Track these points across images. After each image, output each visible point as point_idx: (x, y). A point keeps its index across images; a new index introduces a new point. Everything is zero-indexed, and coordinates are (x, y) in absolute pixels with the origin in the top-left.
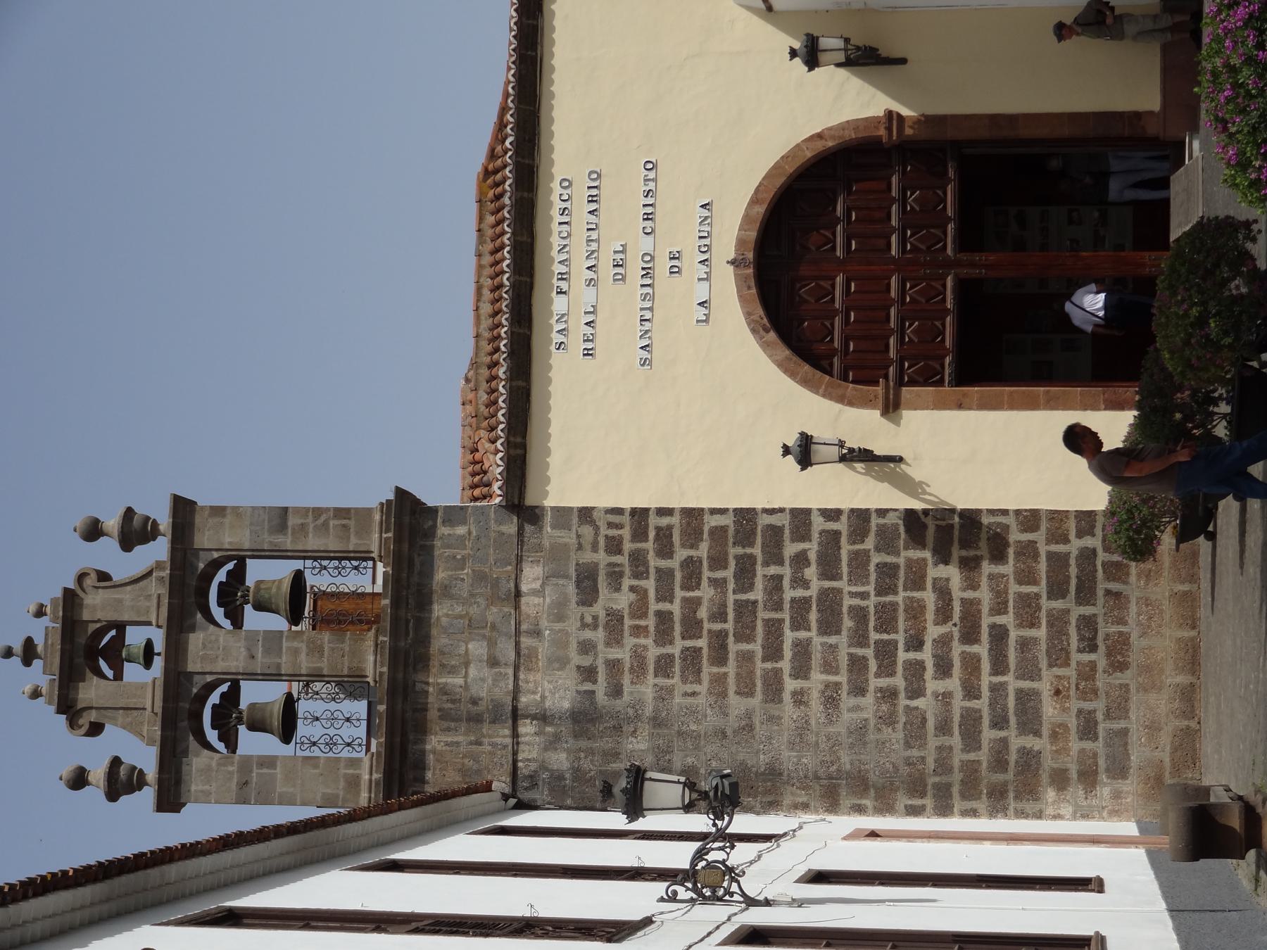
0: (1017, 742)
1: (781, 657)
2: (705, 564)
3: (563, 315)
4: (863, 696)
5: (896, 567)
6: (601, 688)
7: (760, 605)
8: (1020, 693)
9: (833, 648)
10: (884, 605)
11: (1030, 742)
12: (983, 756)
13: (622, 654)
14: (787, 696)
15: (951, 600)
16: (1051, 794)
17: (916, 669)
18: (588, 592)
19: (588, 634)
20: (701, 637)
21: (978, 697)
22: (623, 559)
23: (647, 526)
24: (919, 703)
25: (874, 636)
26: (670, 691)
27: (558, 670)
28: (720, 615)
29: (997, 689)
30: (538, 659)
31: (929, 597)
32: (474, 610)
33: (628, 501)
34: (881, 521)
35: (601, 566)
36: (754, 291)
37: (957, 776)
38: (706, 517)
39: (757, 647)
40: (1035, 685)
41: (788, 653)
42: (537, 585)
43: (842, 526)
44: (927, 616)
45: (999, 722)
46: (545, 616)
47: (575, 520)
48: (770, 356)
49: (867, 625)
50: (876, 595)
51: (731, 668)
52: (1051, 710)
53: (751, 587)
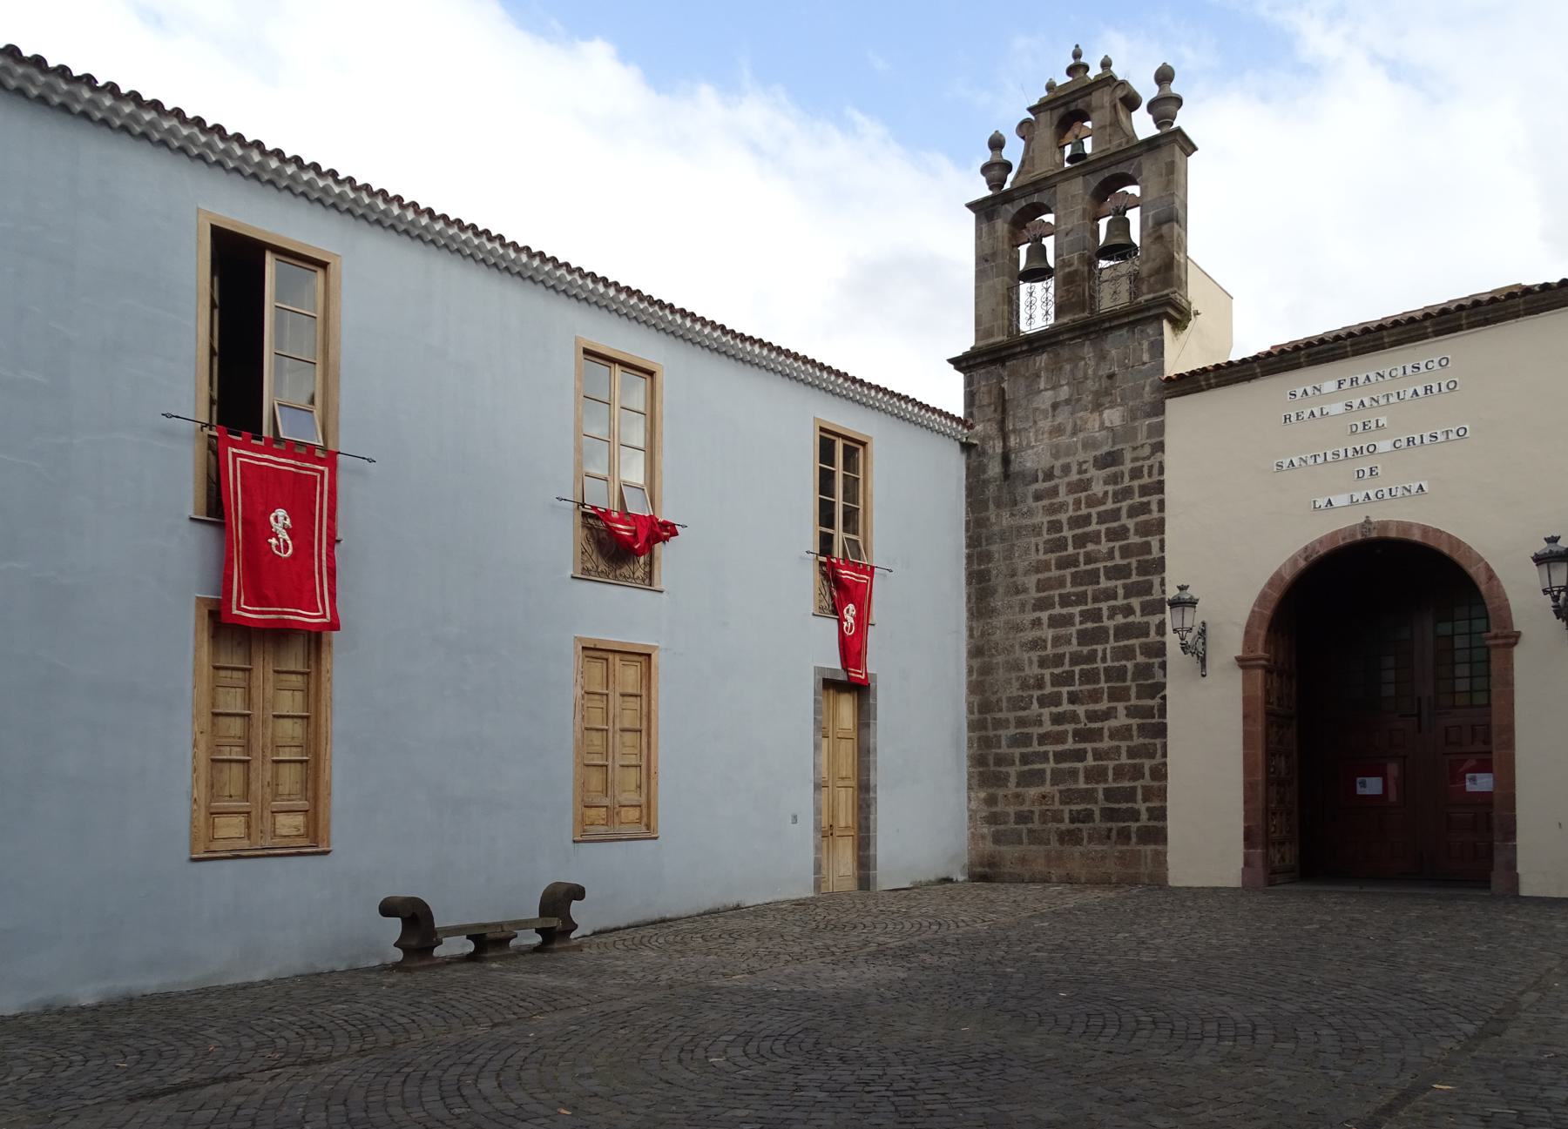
0: (1013, 771)
1: (1062, 607)
2: (1125, 542)
3: (1319, 390)
4: (1039, 666)
5: (1124, 680)
6: (1041, 485)
7: (1096, 587)
8: (1044, 771)
9: (1069, 642)
10: (1098, 674)
11: (1013, 780)
12: (1004, 750)
13: (1063, 496)
14: (1037, 614)
15: (1102, 721)
17: (1055, 700)
18: (1101, 462)
19: (1075, 468)
20: (1074, 548)
21: (1039, 745)
22: (1126, 482)
23: (1150, 495)
24: (1035, 705)
25: (1077, 669)
26: (1039, 534)
27: (1051, 454)
28: (1090, 559)
29: (1044, 757)
30: (1057, 437)
31: (1104, 705)
32: (1089, 383)
33: (1168, 477)
34: (1156, 666)
35: (1121, 467)
36: (1341, 543)
37: (991, 733)
38: (1158, 537)
39: (1069, 589)
40: (1048, 782)
41: (1065, 611)
42: (1107, 424)
43: (1153, 637)
44: (1091, 705)
45: (1025, 759)
46: (1086, 435)
47: (1154, 440)
48: (1285, 564)
49: (1083, 664)
50: (1105, 668)
51: (1055, 573)
52: (1033, 793)
53: (1108, 578)
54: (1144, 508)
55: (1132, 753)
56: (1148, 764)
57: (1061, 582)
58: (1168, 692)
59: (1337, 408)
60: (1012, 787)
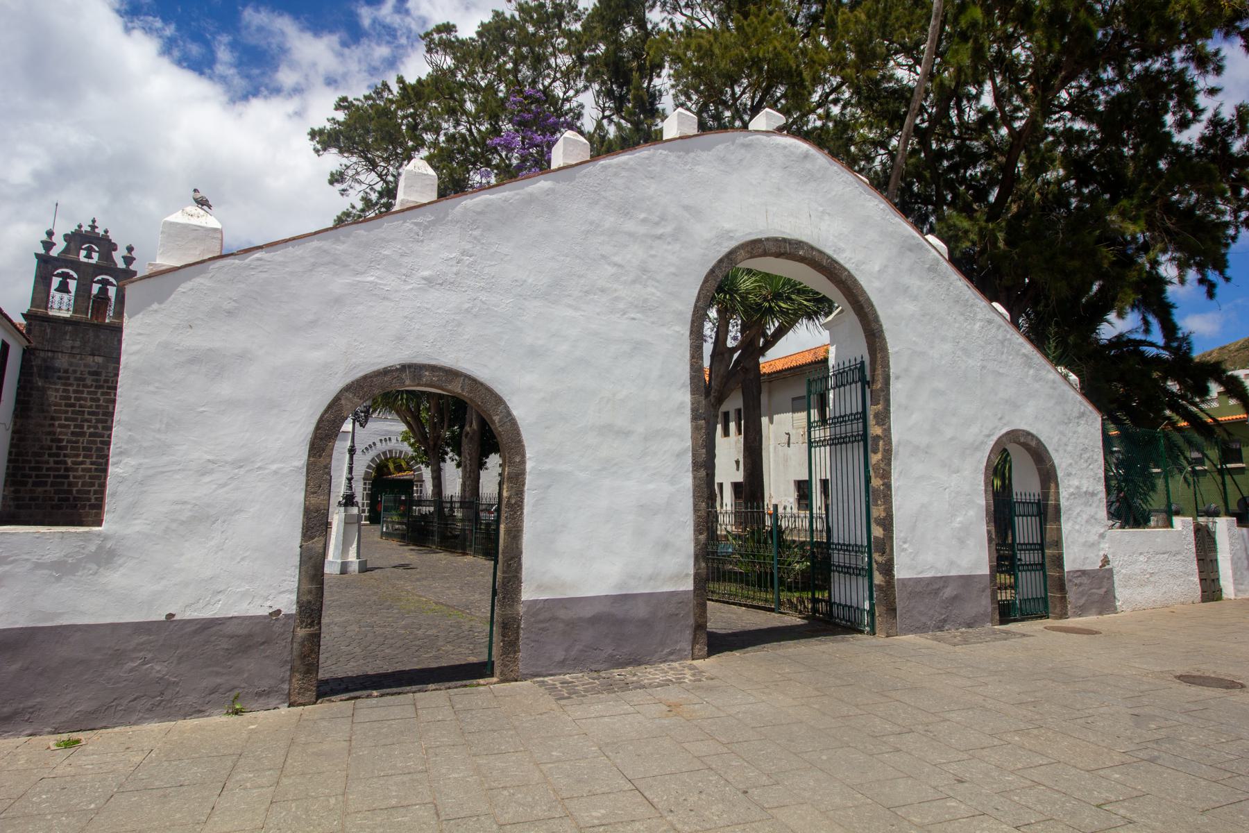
8: (47, 482)
12: (27, 472)
13: (71, 380)
16: (12, 489)
18: (91, 373)
19: (79, 373)
22: (102, 383)
24: (46, 456)
25: (69, 445)
28: (81, 406)
31: (81, 459)
37: (21, 465)
39: (70, 415)
41: (67, 423)
45: (37, 476)
51: (63, 408)
54: (108, 394)
55: (90, 477)
56: (97, 482)
57: (67, 412)
60: (29, 486)
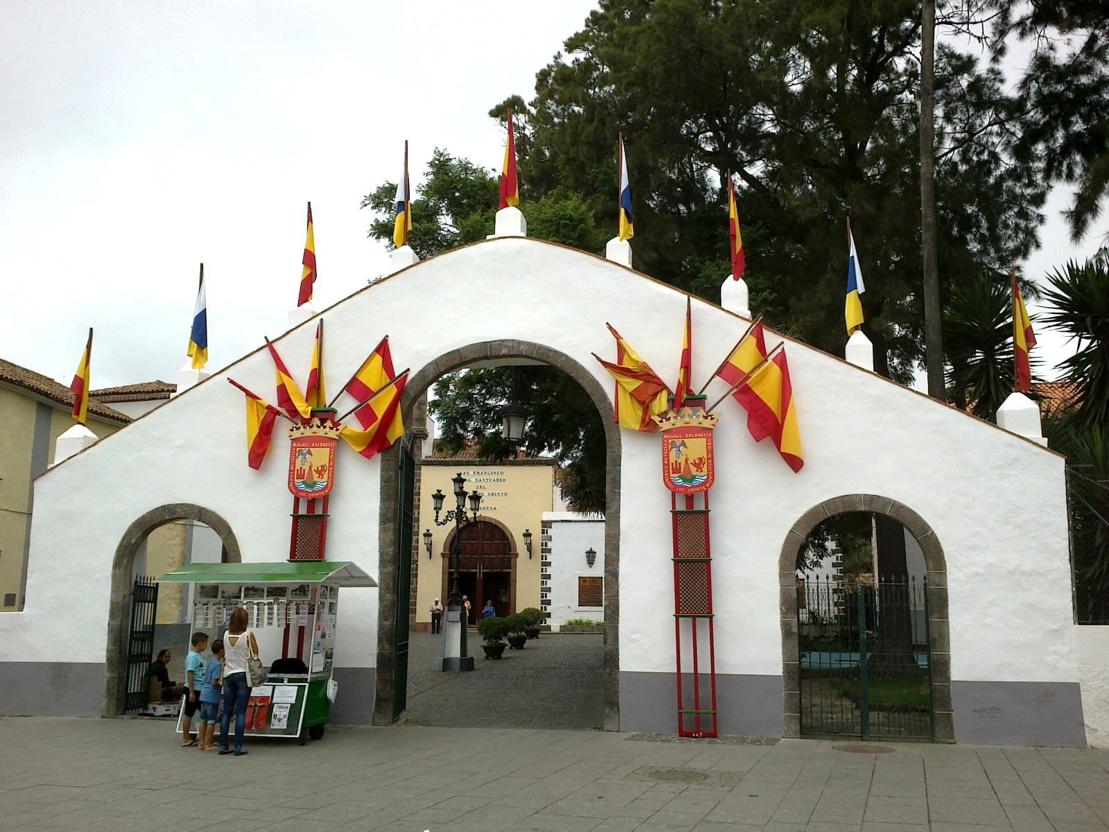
58: (419, 563)
59: (473, 480)
